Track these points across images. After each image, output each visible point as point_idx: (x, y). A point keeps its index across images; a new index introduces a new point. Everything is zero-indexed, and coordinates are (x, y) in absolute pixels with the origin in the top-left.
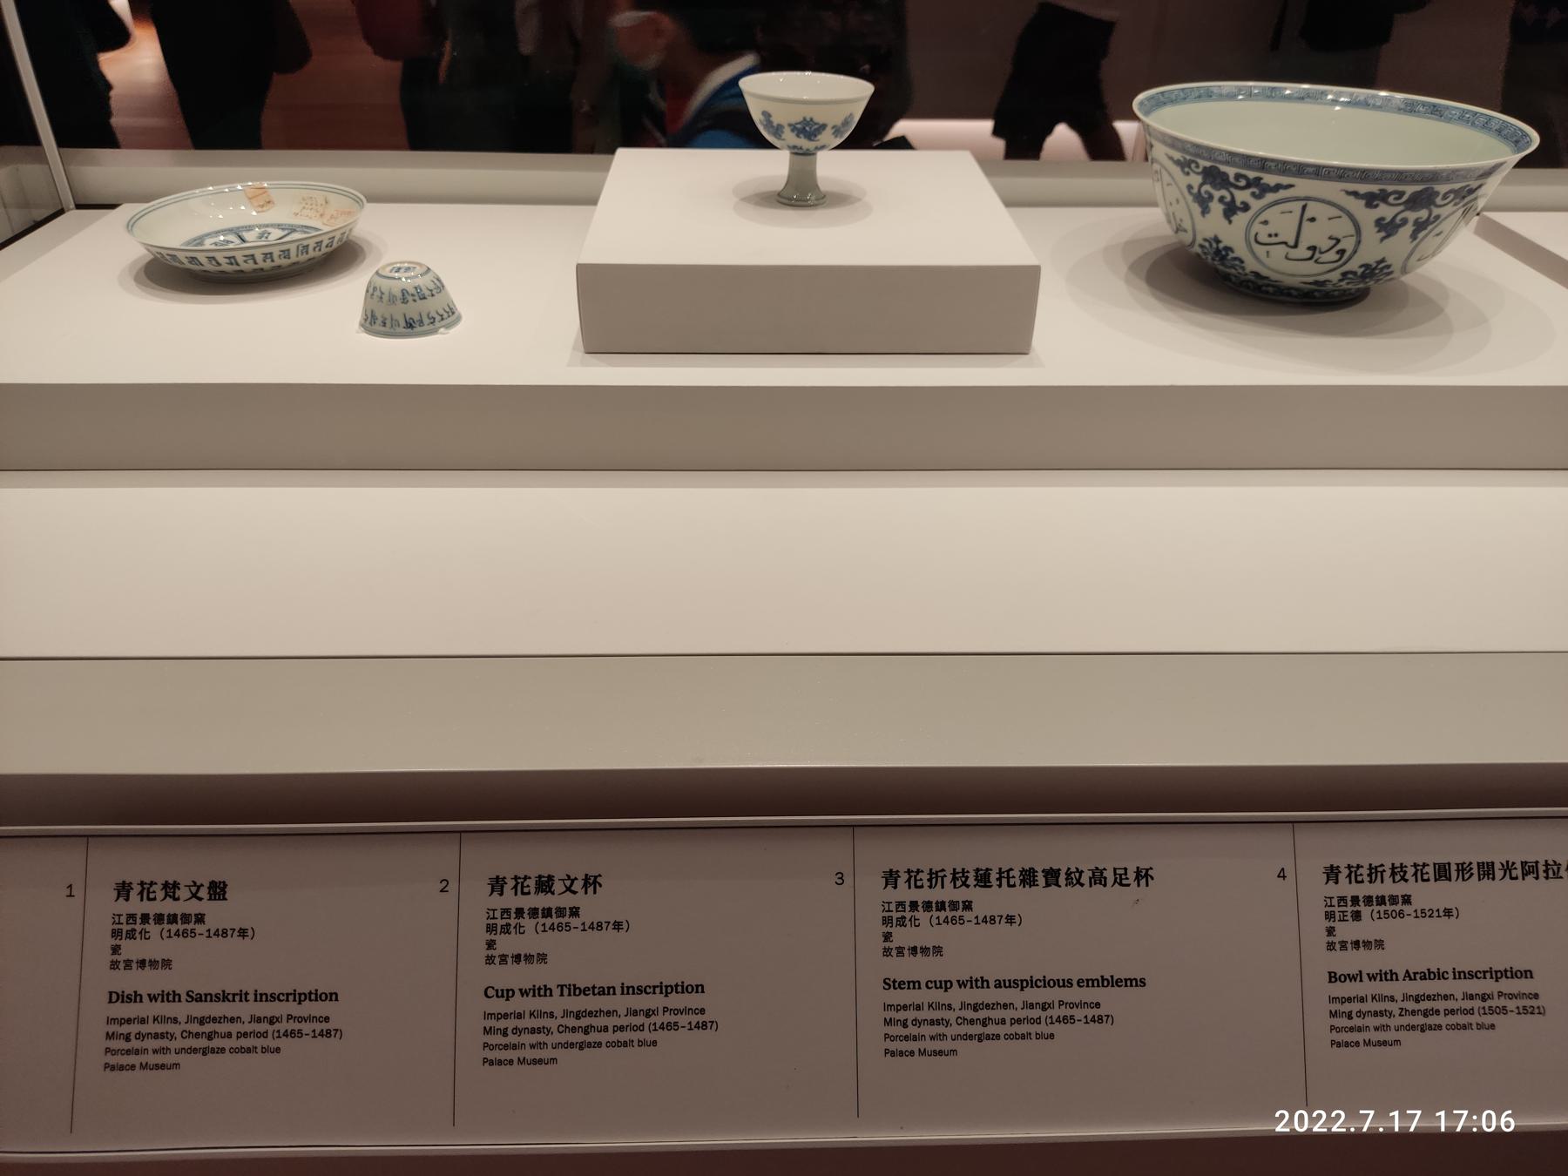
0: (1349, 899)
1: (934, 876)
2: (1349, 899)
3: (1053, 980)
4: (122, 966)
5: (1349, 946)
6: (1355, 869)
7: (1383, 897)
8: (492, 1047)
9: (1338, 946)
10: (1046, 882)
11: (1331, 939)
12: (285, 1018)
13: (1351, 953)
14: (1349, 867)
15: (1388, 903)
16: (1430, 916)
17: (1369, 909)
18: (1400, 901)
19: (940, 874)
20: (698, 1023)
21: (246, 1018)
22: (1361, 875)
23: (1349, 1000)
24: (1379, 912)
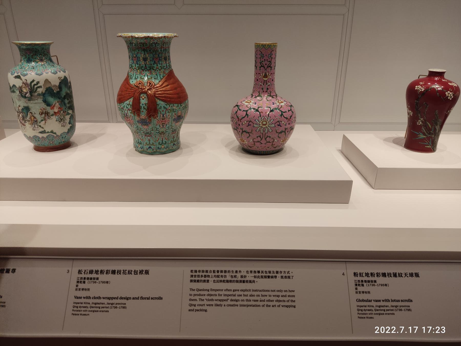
0: (360, 281)
2: (360, 281)
4: (78, 290)
5: (361, 293)
11: (357, 291)
12: (115, 304)
15: (370, 282)
18: (374, 282)
21: (106, 303)
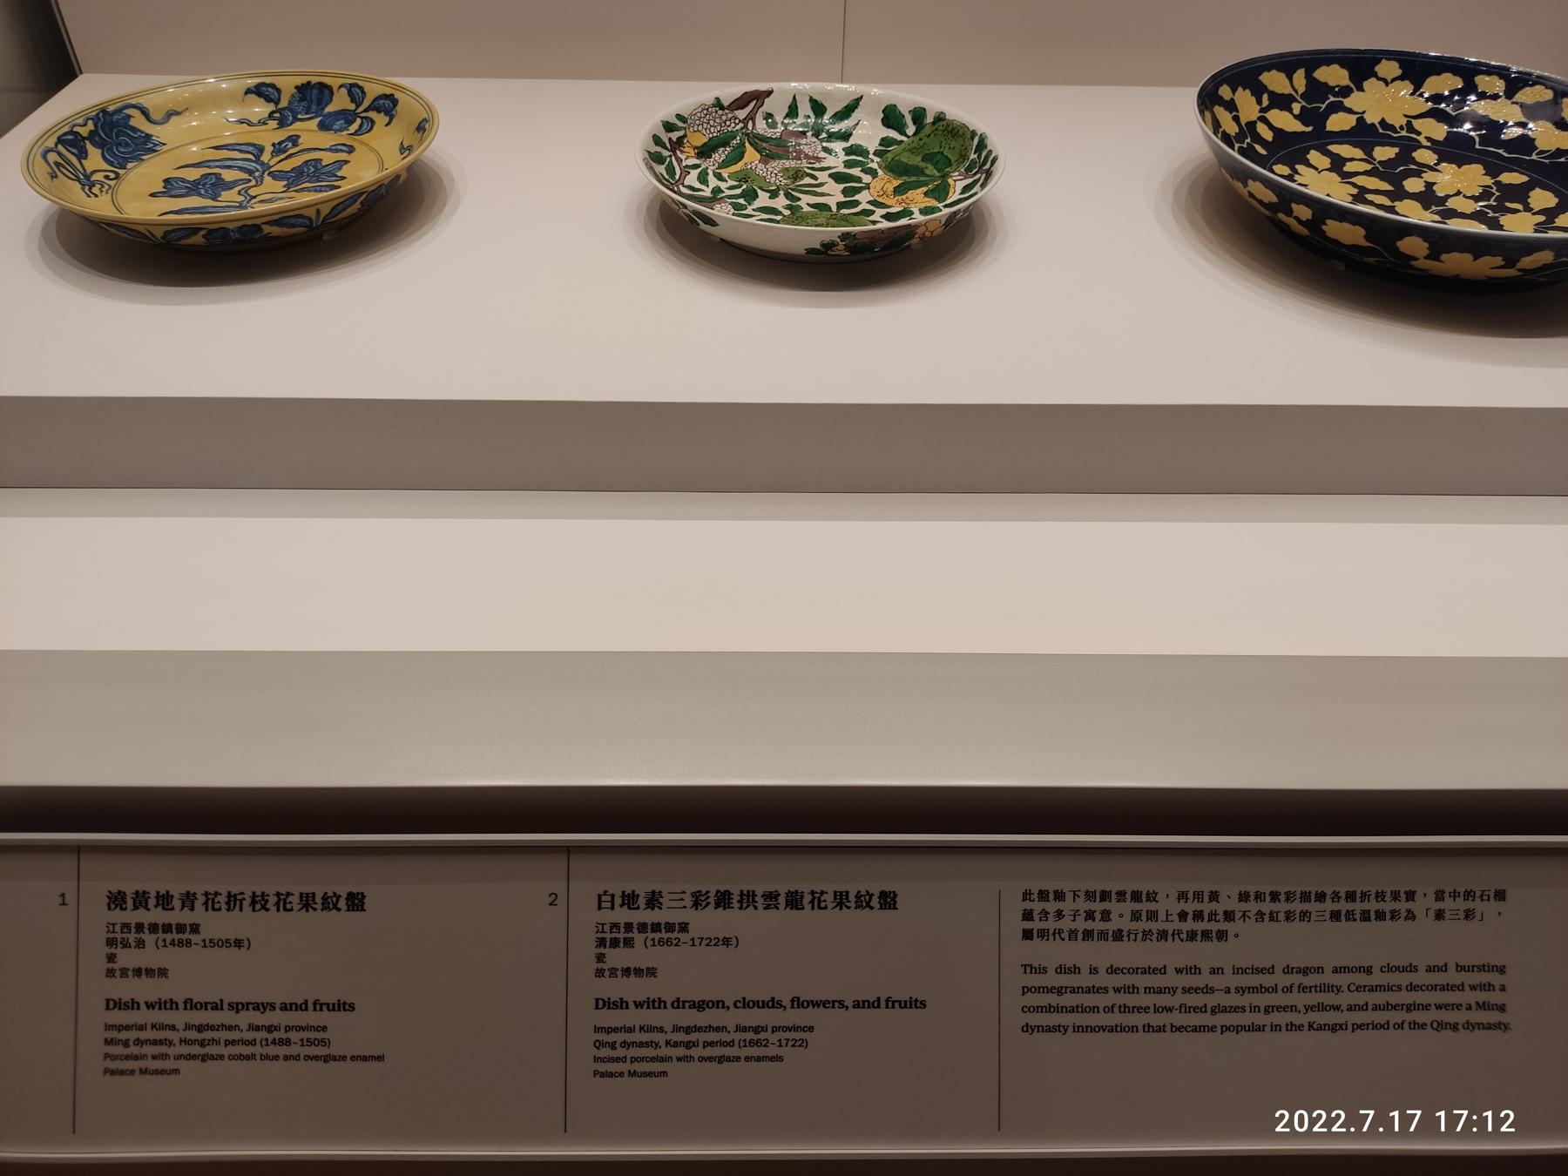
0: (622, 925)
1: (232, 899)
2: (622, 925)
3: (712, 1001)
6: (818, 895)
7: (659, 924)
8: (114, 1058)
9: (607, 973)
10: (134, 905)
11: (600, 965)
13: (621, 980)
14: (206, 894)
15: (663, 930)
16: (675, 945)
17: (643, 936)
19: (238, 897)
20: (274, 1039)
22: (825, 901)
23: (615, 1030)
24: (653, 939)
